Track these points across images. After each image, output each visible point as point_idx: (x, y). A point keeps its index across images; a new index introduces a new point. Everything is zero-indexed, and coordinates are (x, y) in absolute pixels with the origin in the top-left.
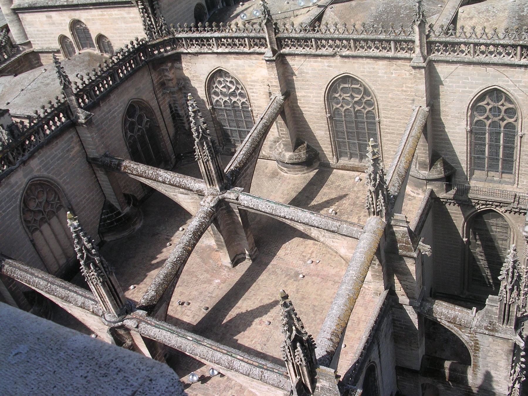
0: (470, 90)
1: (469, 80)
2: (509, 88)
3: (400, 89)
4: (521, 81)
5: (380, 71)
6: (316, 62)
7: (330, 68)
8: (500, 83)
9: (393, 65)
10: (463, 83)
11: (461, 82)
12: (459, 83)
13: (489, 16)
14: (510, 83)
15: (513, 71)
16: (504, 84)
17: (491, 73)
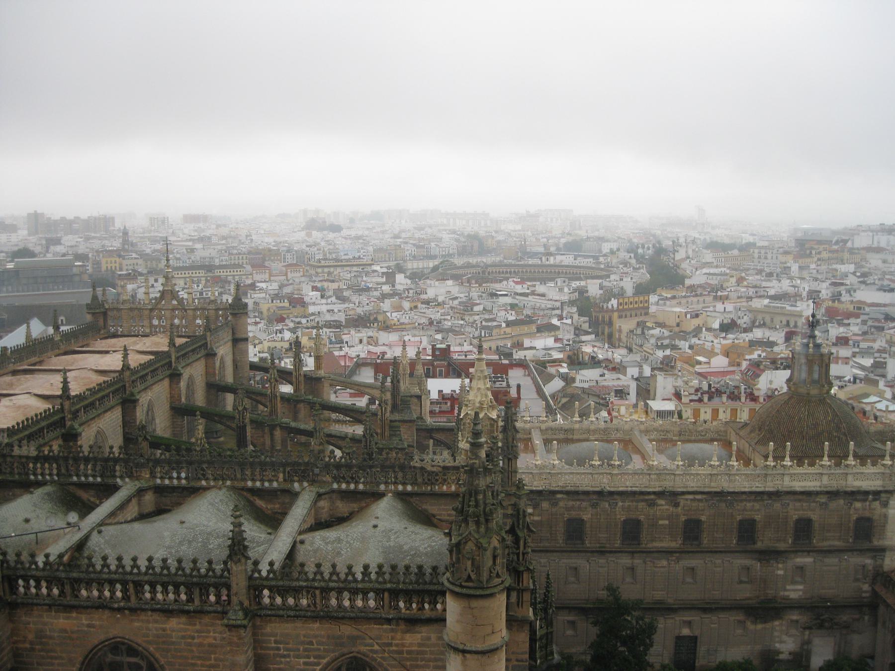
0: (315, 660)
1: (313, 645)
2: (375, 656)
3: (208, 663)
4: (392, 643)
5: (174, 634)
6: (68, 618)
7: (92, 629)
8: (364, 649)
9: (195, 625)
10: (305, 650)
11: (301, 649)
12: (299, 650)
13: (340, 547)
14: (376, 647)
15: (379, 628)
16: (368, 650)
17: (347, 633)
